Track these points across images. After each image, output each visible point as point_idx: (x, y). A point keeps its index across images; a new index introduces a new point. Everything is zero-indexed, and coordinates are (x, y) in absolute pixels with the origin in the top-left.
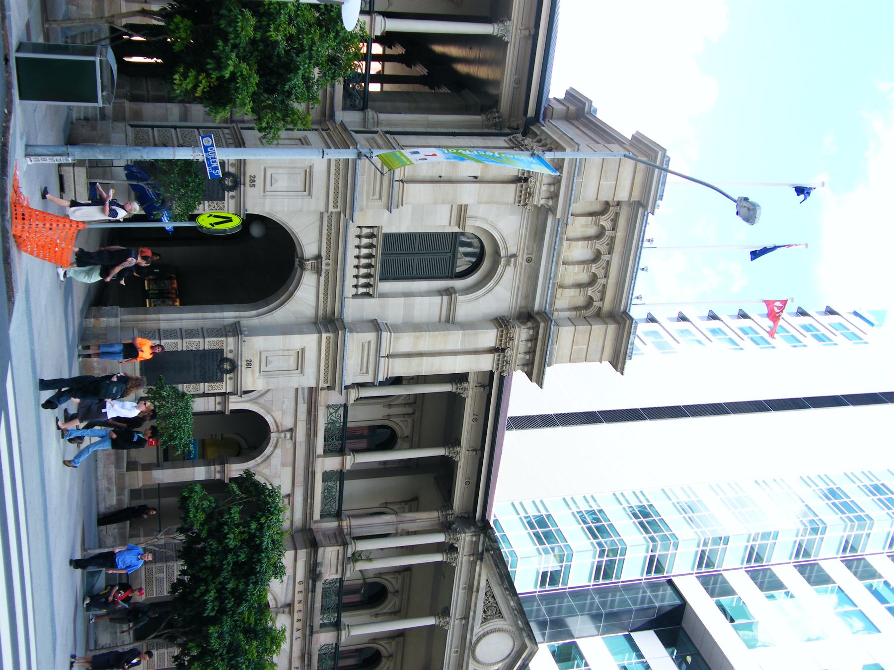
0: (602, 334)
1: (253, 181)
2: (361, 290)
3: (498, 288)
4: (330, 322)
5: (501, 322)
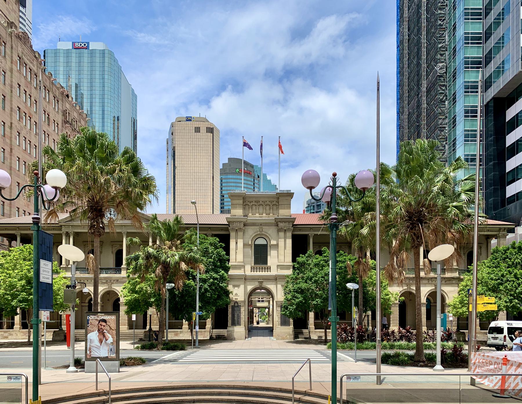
0: (282, 201)
1: (236, 299)
3: (269, 232)
4: (276, 279)
5: (279, 230)
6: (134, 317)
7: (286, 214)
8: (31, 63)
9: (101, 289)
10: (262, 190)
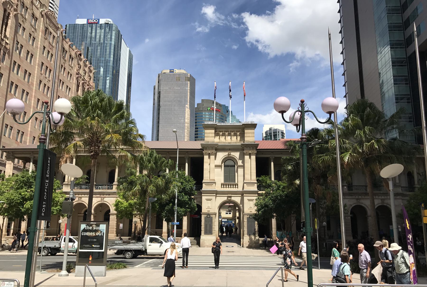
2: (237, 186)
4: (242, 194)
6: (121, 225)
7: (250, 141)
8: (55, 32)
9: (96, 201)
10: (230, 122)
